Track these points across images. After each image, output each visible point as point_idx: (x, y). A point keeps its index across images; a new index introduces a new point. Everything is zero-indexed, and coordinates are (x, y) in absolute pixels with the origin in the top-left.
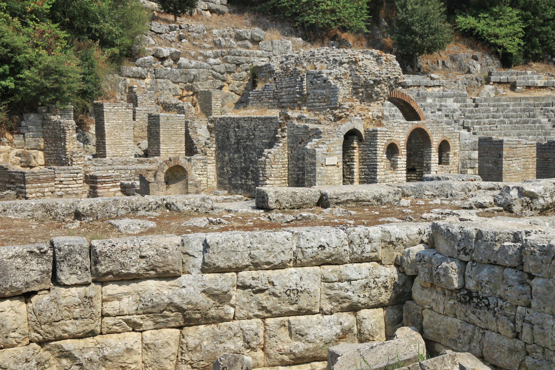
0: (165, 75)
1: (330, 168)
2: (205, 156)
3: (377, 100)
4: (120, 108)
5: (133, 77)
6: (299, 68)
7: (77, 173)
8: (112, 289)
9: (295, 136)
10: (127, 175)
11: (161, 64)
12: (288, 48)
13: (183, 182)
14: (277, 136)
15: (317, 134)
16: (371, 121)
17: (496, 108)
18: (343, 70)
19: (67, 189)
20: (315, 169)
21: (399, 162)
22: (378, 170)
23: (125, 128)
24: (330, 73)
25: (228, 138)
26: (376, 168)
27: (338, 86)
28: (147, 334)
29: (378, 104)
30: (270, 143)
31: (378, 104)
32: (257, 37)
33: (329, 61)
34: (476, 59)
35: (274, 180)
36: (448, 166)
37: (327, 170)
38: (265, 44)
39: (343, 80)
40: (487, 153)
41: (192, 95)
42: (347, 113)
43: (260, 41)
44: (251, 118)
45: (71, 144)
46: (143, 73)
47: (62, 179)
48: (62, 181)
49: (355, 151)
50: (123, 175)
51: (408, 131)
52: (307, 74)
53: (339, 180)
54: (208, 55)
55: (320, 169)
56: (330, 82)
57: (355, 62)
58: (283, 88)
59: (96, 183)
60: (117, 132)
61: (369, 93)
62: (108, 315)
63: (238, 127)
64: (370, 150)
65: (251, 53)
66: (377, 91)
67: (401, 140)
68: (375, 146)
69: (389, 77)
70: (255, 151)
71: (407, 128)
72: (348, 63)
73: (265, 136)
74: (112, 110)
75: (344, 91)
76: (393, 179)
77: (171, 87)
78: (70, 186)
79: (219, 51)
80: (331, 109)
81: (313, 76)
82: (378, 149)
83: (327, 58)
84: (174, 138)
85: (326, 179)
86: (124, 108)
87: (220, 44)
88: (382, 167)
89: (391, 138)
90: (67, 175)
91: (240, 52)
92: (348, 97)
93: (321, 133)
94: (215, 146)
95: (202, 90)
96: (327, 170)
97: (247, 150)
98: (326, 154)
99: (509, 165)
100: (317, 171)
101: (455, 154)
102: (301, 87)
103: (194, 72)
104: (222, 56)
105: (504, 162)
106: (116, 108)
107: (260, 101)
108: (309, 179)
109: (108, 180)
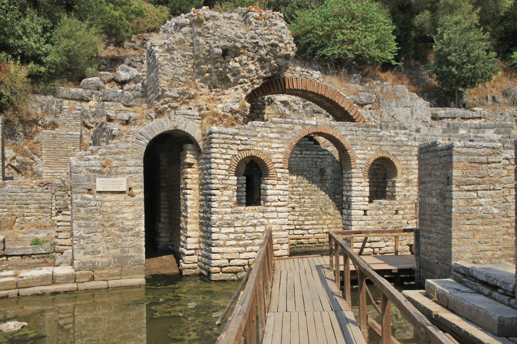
1: (109, 197)
3: (236, 83)
5: (72, 99)
16: (220, 119)
21: (269, 192)
36: (392, 202)
37: (104, 202)
40: (430, 175)
46: (84, 94)
55: (83, 198)
61: (221, 72)
66: (234, 68)
71: (290, 132)
76: (255, 221)
82: (214, 166)
85: (100, 217)
88: (227, 198)
89: (248, 147)
92: (183, 79)
96: (104, 202)
99: (468, 200)
101: (408, 182)
105: (455, 194)
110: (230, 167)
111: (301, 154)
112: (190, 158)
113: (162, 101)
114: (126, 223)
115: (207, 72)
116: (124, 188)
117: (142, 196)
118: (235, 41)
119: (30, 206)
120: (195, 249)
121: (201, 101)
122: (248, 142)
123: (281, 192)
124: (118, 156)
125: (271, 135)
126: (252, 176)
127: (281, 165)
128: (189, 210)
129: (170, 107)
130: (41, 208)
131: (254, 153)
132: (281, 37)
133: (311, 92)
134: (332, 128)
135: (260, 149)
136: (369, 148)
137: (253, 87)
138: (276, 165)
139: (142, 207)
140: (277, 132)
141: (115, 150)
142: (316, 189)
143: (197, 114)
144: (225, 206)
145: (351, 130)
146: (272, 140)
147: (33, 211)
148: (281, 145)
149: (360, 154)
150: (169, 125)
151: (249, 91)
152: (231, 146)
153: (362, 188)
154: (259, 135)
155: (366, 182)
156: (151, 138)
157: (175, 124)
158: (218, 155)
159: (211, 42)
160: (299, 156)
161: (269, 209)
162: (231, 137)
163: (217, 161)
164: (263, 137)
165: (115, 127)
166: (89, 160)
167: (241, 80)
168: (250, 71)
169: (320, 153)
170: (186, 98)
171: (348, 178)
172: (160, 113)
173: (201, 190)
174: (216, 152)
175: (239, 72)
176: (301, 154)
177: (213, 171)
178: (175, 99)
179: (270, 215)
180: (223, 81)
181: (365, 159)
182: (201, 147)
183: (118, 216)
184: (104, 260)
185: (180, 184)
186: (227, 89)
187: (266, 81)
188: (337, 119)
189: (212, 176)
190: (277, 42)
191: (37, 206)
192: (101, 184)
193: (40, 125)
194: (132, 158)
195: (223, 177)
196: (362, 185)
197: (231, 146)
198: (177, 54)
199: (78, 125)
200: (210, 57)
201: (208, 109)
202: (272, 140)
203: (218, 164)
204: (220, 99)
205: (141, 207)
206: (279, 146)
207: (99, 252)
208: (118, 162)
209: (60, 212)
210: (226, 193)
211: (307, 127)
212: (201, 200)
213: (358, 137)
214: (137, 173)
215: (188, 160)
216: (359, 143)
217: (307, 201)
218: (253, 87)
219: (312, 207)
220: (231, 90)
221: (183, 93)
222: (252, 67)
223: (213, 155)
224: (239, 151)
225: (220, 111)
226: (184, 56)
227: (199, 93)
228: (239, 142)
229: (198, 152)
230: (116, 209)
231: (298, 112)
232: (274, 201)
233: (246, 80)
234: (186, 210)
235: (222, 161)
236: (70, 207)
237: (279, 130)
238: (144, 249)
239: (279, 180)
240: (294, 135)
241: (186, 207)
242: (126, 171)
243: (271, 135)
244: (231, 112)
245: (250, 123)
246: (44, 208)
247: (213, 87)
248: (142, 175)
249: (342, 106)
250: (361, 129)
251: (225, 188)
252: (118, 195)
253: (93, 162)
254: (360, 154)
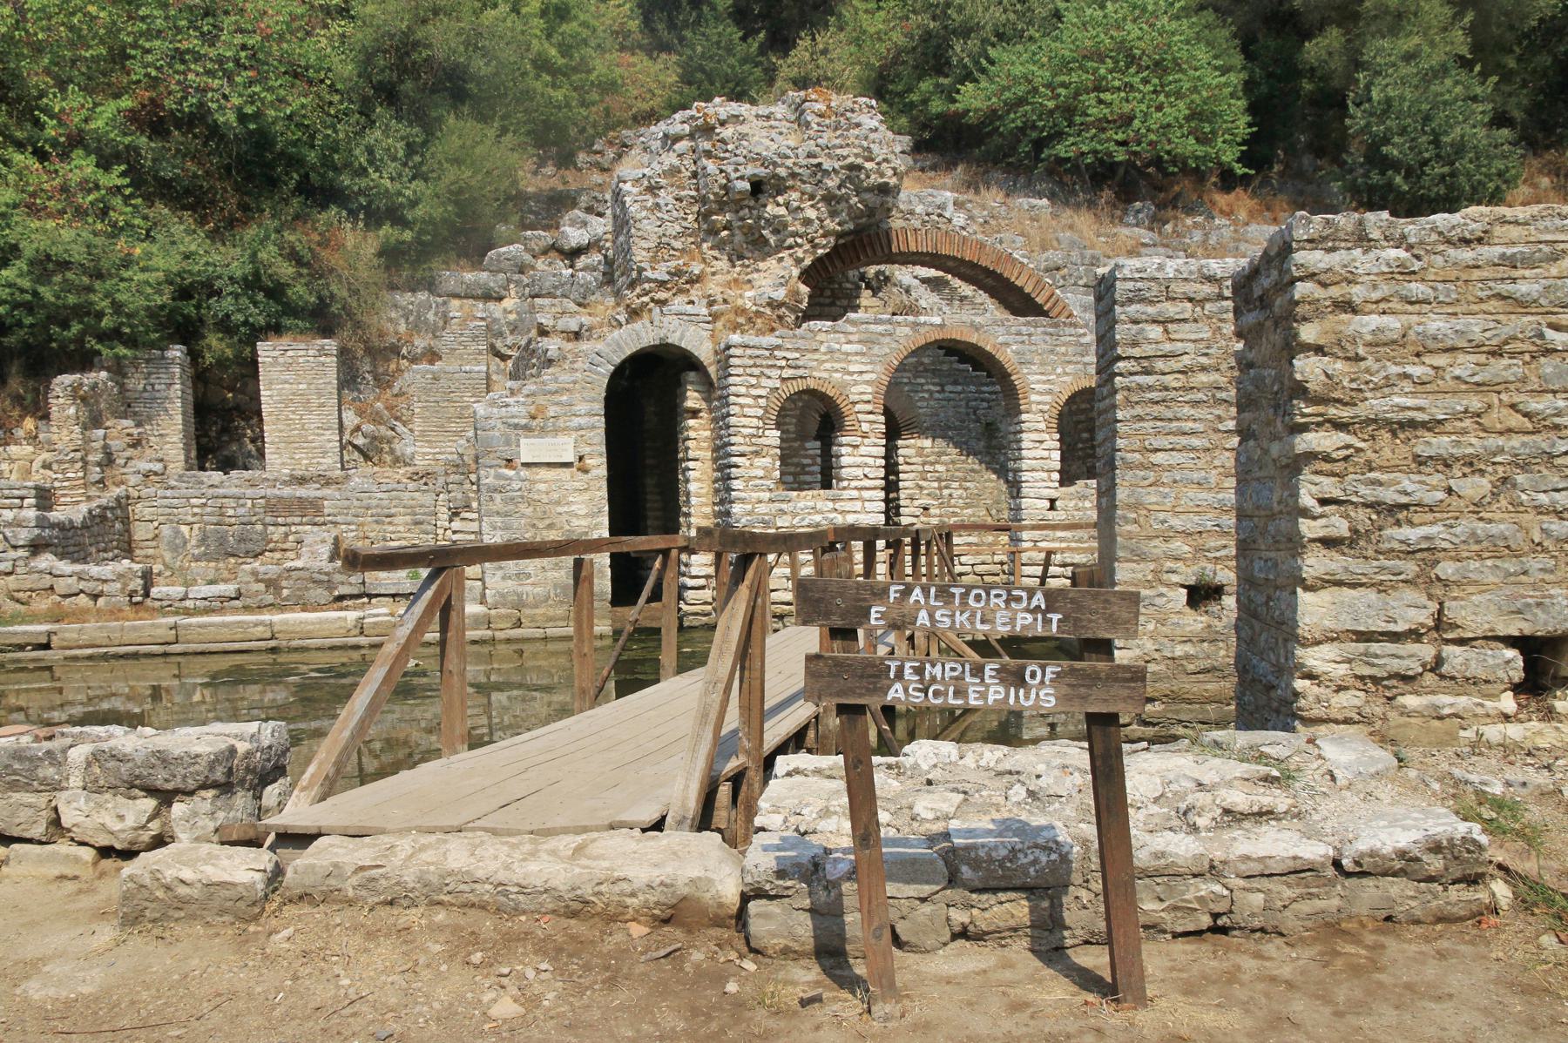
0: (555, 287)
1: (544, 473)
3: (780, 247)
5: (467, 297)
7: (22, 498)
10: (241, 511)
21: (844, 461)
23: (315, 401)
29: (781, 259)
37: (534, 482)
45: (65, 432)
50: (231, 512)
55: (498, 477)
61: (750, 227)
66: (775, 217)
82: (734, 410)
88: (761, 473)
89: (800, 372)
92: (677, 244)
96: (534, 482)
110: (766, 411)
111: (943, 391)
112: (693, 399)
113: (638, 290)
114: (575, 522)
115: (725, 228)
116: (569, 457)
117: (603, 471)
118: (775, 164)
119: (396, 520)
120: (707, 577)
121: (713, 287)
122: (800, 363)
123: (870, 461)
124: (557, 398)
125: (847, 348)
126: (813, 426)
127: (869, 407)
128: (693, 500)
129: (652, 300)
130: (417, 523)
131: (812, 384)
132: (868, 149)
133: (948, 257)
134: (977, 329)
135: (825, 375)
136: (1059, 370)
137: (814, 253)
138: (858, 407)
139: (604, 493)
140: (860, 342)
141: (552, 387)
142: (976, 467)
143: (704, 311)
144: (757, 488)
145: (1019, 334)
146: (853, 359)
147: (401, 528)
148: (869, 368)
149: (1038, 382)
150: (651, 335)
151: (808, 262)
152: (767, 371)
153: (1045, 454)
154: (823, 349)
155: (1052, 441)
156: (618, 361)
157: (662, 333)
158: (743, 390)
159: (730, 169)
160: (937, 395)
161: (846, 494)
162: (767, 353)
163: (741, 400)
164: (831, 351)
165: (552, 345)
166: (507, 406)
167: (790, 241)
168: (807, 222)
169: (985, 389)
170: (684, 281)
171: (1016, 433)
172: (634, 313)
173: (715, 460)
174: (738, 384)
175: (785, 226)
176: (943, 391)
177: (733, 420)
178: (662, 284)
179: (848, 506)
180: (755, 244)
181: (1050, 392)
182: (713, 376)
183: (560, 509)
184: (538, 590)
185: (677, 452)
186: (763, 260)
187: (850, 238)
188: (1016, 312)
189: (732, 430)
190: (859, 161)
191: (408, 518)
192: (530, 449)
193: (404, 357)
194: (584, 400)
195: (753, 431)
196: (1044, 446)
197: (767, 371)
198: (665, 197)
199: (480, 353)
200: (728, 200)
201: (725, 301)
202: (853, 359)
203: (742, 406)
204: (749, 281)
205: (602, 493)
206: (864, 368)
207: (529, 576)
208: (558, 409)
209: (456, 514)
210: (759, 461)
211: (922, 330)
212: (715, 481)
213: (1033, 348)
214: (594, 427)
215: (690, 404)
216: (1037, 359)
217: (956, 493)
218: (814, 253)
219: (968, 506)
220: (771, 262)
221: (678, 273)
222: (811, 214)
223: (733, 389)
224: (784, 380)
225: (749, 305)
226: (679, 199)
227: (709, 270)
228: (783, 363)
229: (709, 388)
230: (556, 496)
231: (973, 303)
232: (856, 478)
233: (799, 241)
234: (688, 501)
235: (749, 401)
236: (475, 505)
237: (863, 336)
238: (609, 571)
239: (865, 436)
240: (894, 345)
241: (688, 494)
242: (572, 424)
243: (847, 348)
244: (769, 304)
245: (805, 325)
246: (421, 523)
247: (736, 256)
248: (602, 432)
249: (1019, 283)
250: (1040, 330)
251: (757, 454)
252: (559, 470)
253: (514, 410)
254: (1038, 382)
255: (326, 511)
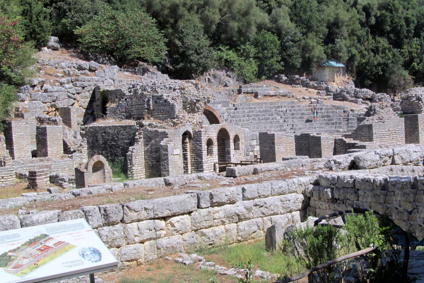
1: (176, 156)
2: (81, 154)
4: (22, 124)
6: (145, 93)
7: (12, 171)
8: (216, 208)
9: (149, 137)
11: (33, 90)
12: (115, 74)
13: (101, 171)
14: (136, 137)
15: (165, 135)
17: (248, 110)
18: (177, 94)
19: (7, 182)
20: (168, 158)
21: (214, 150)
22: (203, 156)
24: (168, 96)
25: (97, 140)
26: (202, 155)
27: (175, 104)
28: (227, 225)
30: (130, 142)
31: (199, 114)
32: (93, 68)
33: (167, 88)
34: (230, 77)
35: (138, 167)
38: (100, 72)
39: (177, 100)
41: (55, 111)
42: (182, 121)
43: (96, 70)
44: (115, 126)
47: (3, 176)
48: (3, 177)
49: (187, 144)
51: (217, 130)
52: (152, 97)
53: (181, 164)
54: (63, 81)
55: (171, 158)
56: (169, 102)
57: (184, 89)
58: (133, 105)
59: (36, 176)
60: (20, 141)
62: (215, 219)
63: (105, 133)
64: (197, 144)
65: (91, 79)
67: (214, 136)
68: (200, 141)
69: (204, 97)
70: (119, 148)
72: (179, 89)
73: (126, 138)
74: (17, 126)
75: (178, 107)
77: (42, 106)
78: (8, 180)
79: (69, 78)
80: (171, 119)
81: (156, 98)
83: (165, 86)
84: (56, 143)
86: (24, 123)
87: (69, 73)
90: (6, 173)
91: (84, 78)
93: (167, 134)
94: (86, 146)
95: (62, 106)
97: (113, 148)
98: (173, 148)
99: (278, 148)
100: (169, 158)
101: (242, 143)
102: (149, 105)
103: (56, 94)
104: (72, 82)
105: (276, 147)
106: (19, 124)
107: (115, 114)
108: (164, 164)
109: (42, 173)
255: (52, 168)
